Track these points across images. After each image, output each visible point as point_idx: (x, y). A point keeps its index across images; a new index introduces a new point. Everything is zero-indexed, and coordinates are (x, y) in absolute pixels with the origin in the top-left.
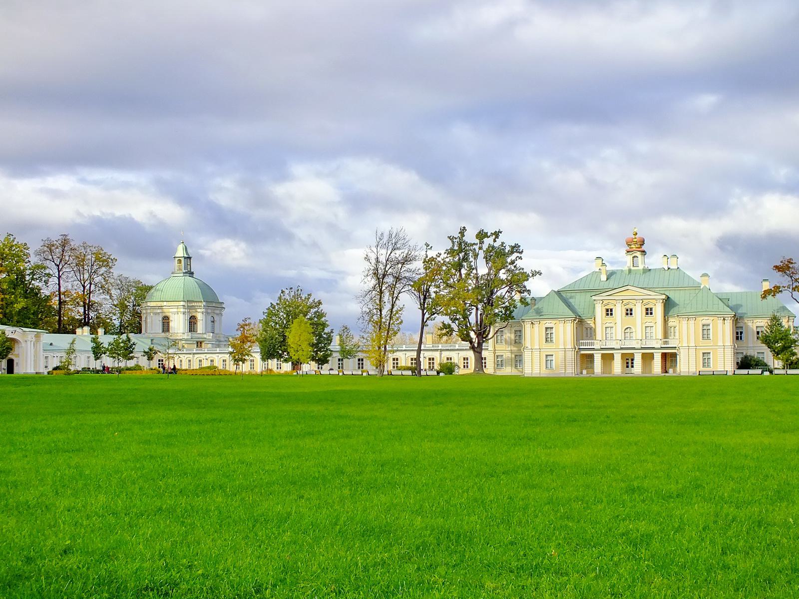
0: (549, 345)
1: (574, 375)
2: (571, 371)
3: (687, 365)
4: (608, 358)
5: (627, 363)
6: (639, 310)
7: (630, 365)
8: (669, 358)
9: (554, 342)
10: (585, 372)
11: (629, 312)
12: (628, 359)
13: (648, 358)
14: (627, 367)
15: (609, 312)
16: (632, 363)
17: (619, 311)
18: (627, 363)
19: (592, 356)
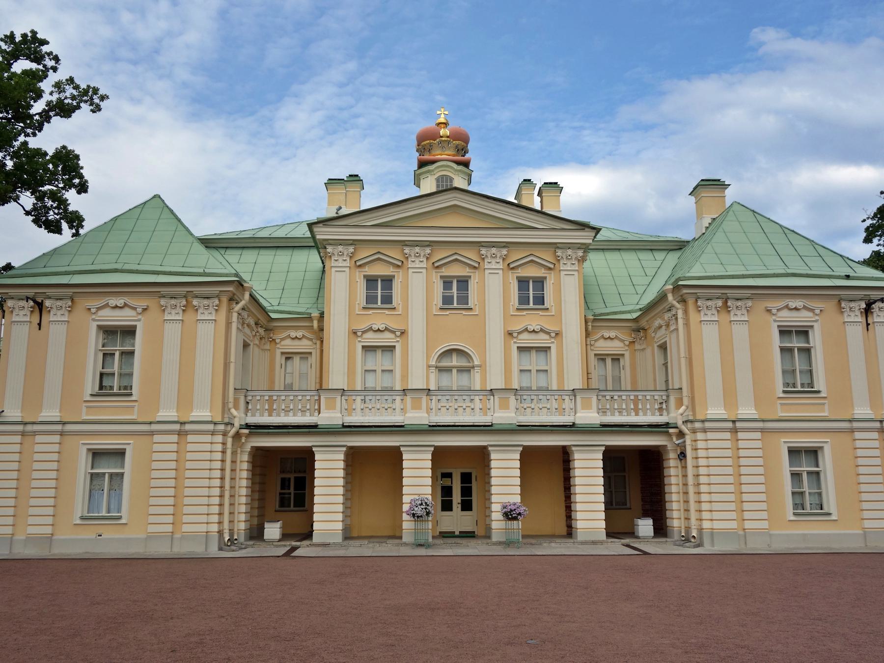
0: (111, 410)
1: (213, 550)
2: (203, 528)
3: (727, 501)
4: (371, 466)
5: (447, 491)
6: (493, 288)
7: (457, 498)
8: (639, 478)
9: (134, 391)
10: (272, 531)
11: (456, 293)
12: (449, 475)
13: (548, 466)
14: (447, 506)
15: (379, 290)
16: (466, 492)
17: (417, 287)
18: (447, 491)
19: (306, 458)
